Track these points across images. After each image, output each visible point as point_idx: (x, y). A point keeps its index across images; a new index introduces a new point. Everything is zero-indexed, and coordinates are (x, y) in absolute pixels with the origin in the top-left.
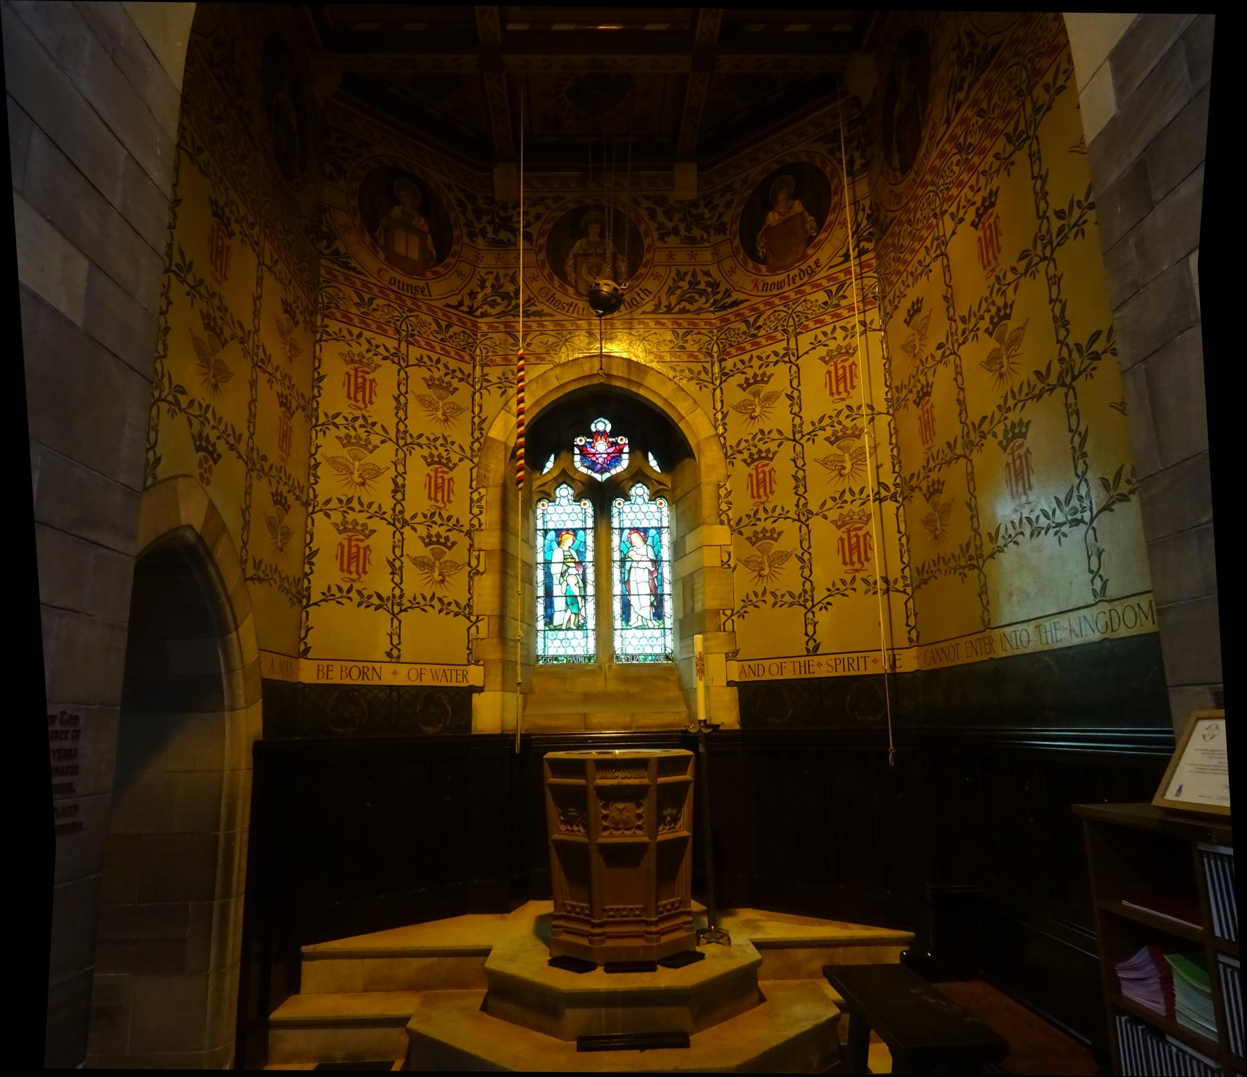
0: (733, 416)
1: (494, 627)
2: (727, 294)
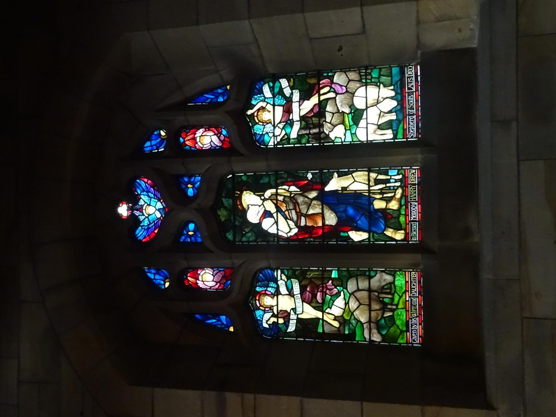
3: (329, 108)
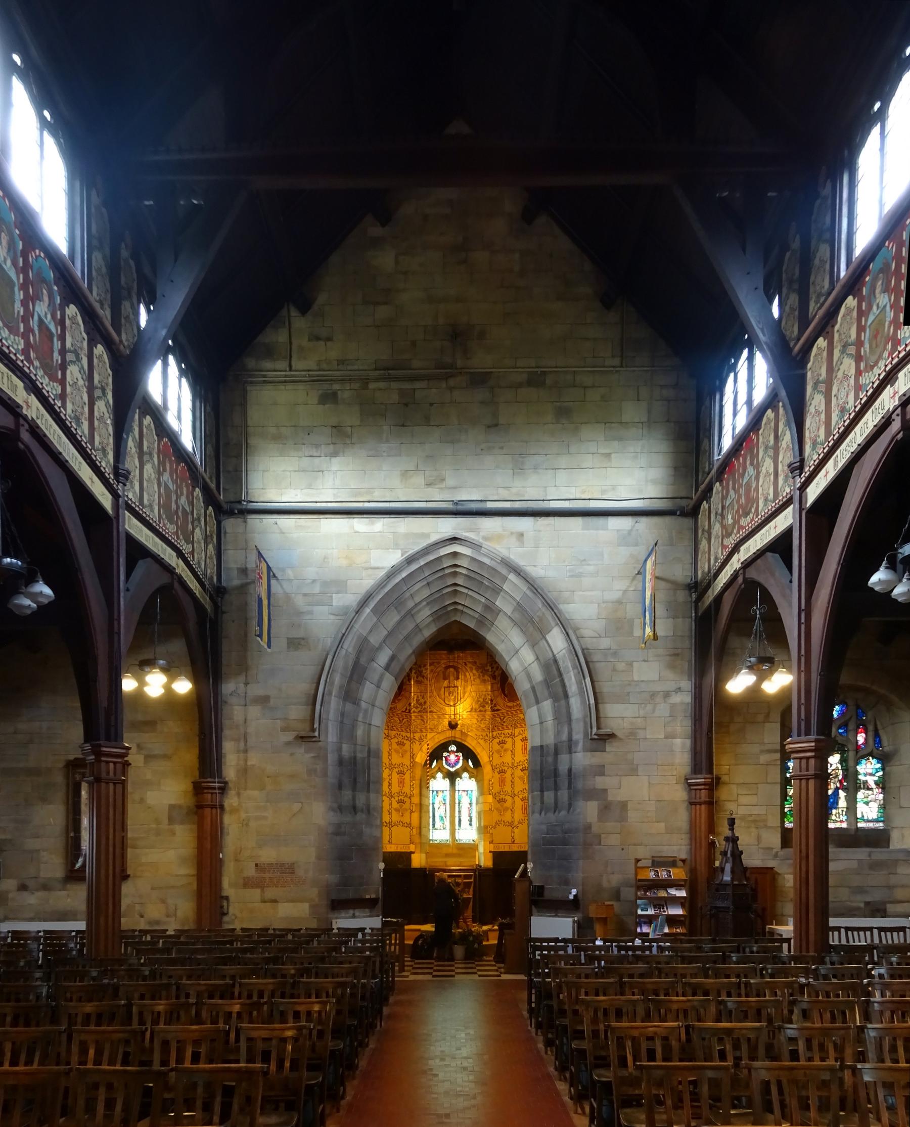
0: (495, 754)
1: (418, 831)
2: (495, 706)
3: (870, 792)
